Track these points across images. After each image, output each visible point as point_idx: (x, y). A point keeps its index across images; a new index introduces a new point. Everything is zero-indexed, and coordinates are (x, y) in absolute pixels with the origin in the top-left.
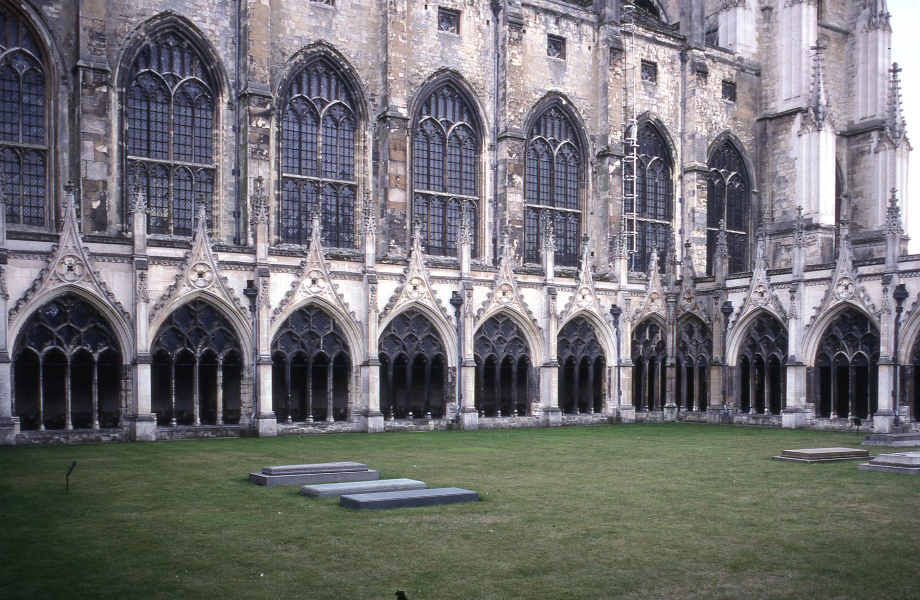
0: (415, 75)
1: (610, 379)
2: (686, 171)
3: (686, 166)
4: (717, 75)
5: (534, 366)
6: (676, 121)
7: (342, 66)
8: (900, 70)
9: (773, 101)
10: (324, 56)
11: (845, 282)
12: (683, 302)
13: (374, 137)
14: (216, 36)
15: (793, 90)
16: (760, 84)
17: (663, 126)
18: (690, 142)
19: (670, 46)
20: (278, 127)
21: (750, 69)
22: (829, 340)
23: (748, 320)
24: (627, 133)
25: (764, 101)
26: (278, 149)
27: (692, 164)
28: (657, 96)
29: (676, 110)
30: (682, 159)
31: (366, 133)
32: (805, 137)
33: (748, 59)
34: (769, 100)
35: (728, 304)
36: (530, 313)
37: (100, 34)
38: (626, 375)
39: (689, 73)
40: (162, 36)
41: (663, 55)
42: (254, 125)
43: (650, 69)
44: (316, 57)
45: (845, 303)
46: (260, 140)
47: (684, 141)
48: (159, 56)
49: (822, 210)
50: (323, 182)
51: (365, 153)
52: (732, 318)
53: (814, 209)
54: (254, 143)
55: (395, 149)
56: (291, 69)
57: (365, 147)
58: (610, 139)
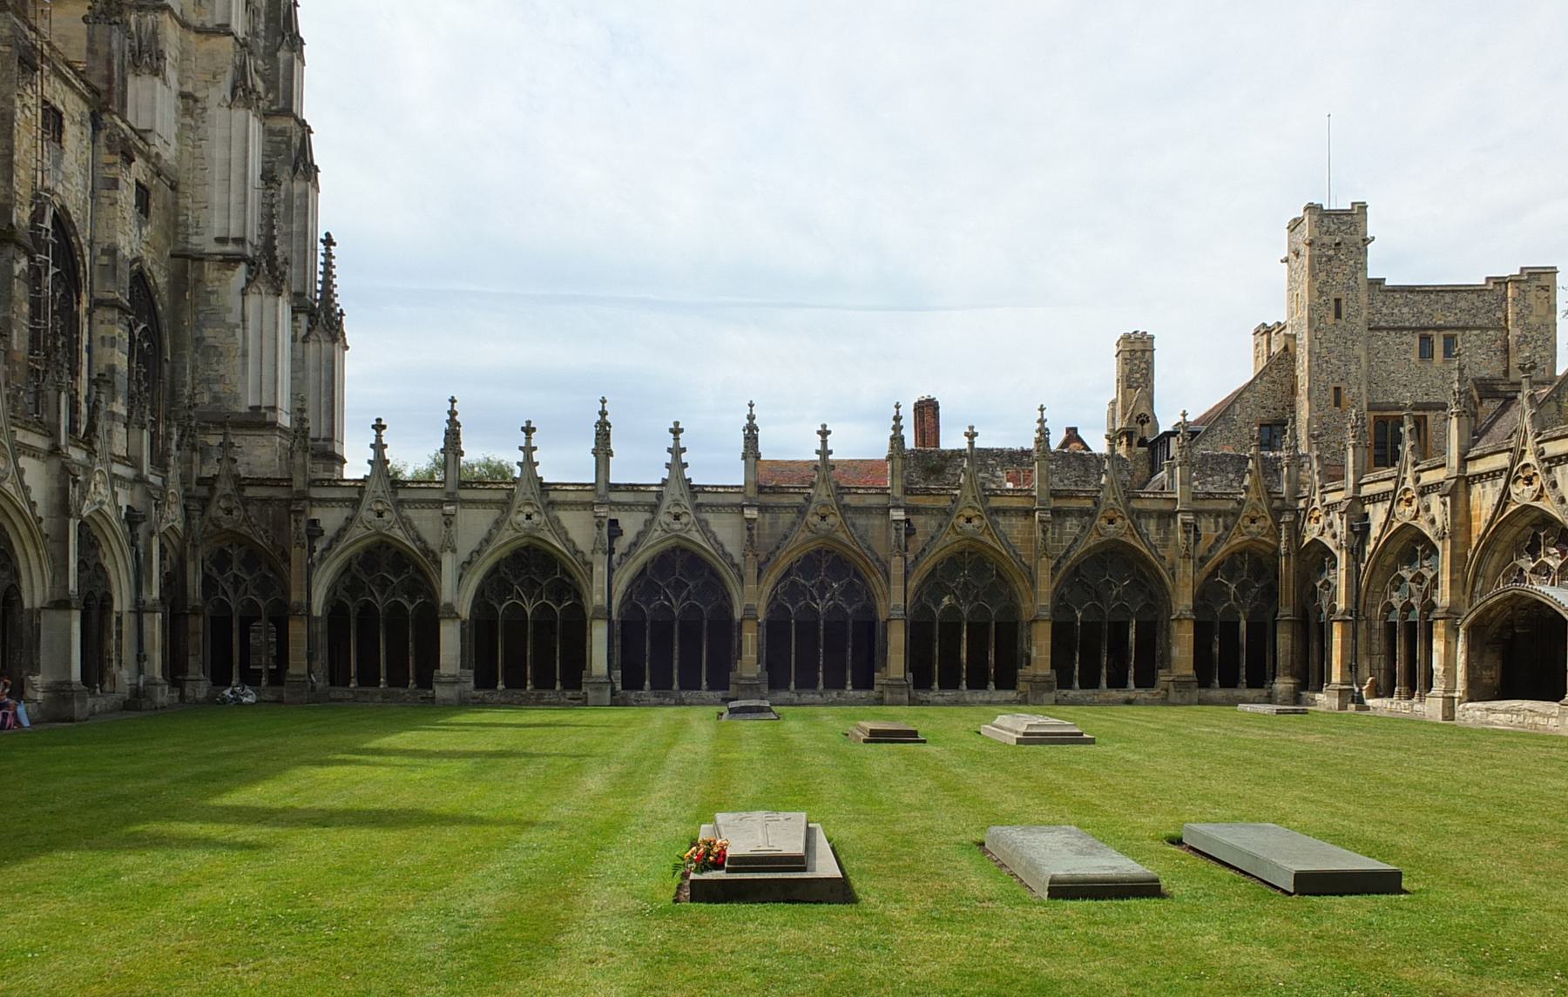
1: (119, 634)
2: (96, 304)
3: (97, 295)
4: (139, 169)
5: (27, 605)
6: (85, 220)
8: (334, 244)
9: (197, 234)
11: (528, 510)
12: (215, 511)
15: (232, 227)
16: (176, 204)
17: (70, 221)
18: (105, 260)
19: (82, 96)
21: (166, 176)
22: (496, 583)
23: (352, 549)
24: (37, 217)
25: (181, 229)
27: (111, 296)
28: (62, 167)
29: (85, 202)
30: (91, 283)
32: (252, 301)
33: (166, 161)
34: (191, 231)
35: (314, 522)
36: (33, 505)
38: (154, 626)
39: (104, 150)
41: (72, 106)
43: (53, 120)
45: (529, 536)
47: (93, 258)
49: (279, 406)
52: (320, 546)
53: (267, 402)
58: (14, 215)
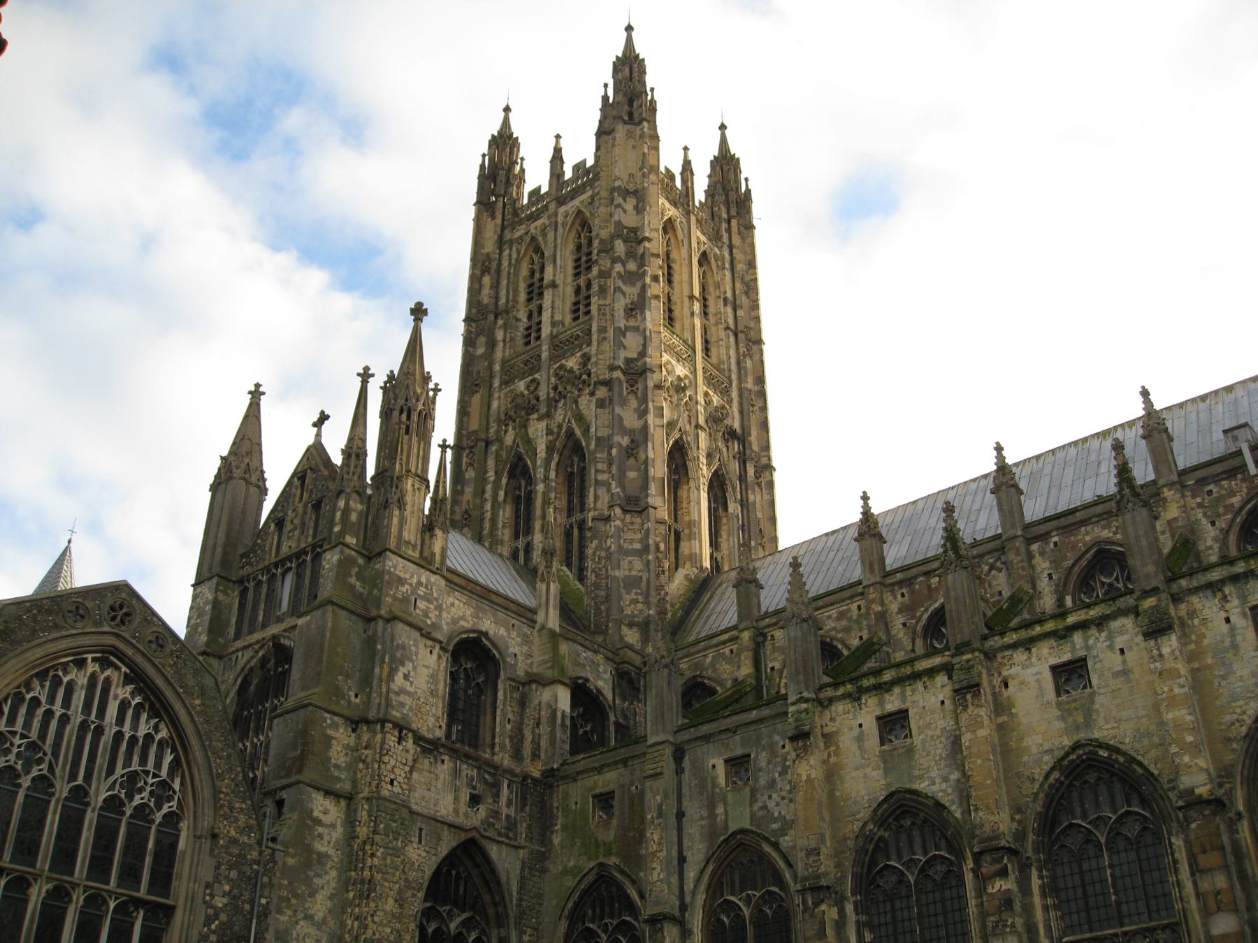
0: (1233, 724)
7: (1116, 761)
10: (1088, 759)
13: (1186, 841)
14: (948, 795)
20: (1041, 877)
26: (1046, 908)
31: (1173, 840)
37: (815, 849)
40: (895, 819)
42: (990, 890)
44: (1078, 765)
46: (1000, 907)
48: (898, 842)
50: (1125, 933)
51: (1176, 870)
54: (993, 915)
55: (1204, 852)
56: (1046, 796)
57: (1175, 862)
